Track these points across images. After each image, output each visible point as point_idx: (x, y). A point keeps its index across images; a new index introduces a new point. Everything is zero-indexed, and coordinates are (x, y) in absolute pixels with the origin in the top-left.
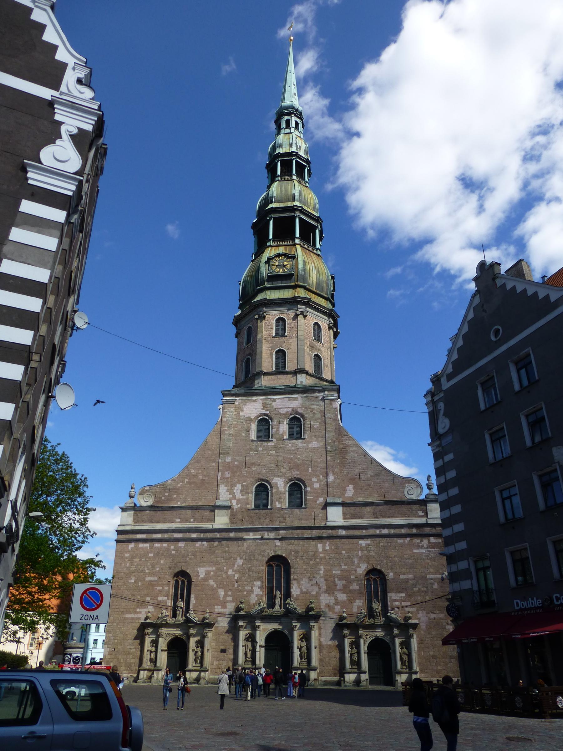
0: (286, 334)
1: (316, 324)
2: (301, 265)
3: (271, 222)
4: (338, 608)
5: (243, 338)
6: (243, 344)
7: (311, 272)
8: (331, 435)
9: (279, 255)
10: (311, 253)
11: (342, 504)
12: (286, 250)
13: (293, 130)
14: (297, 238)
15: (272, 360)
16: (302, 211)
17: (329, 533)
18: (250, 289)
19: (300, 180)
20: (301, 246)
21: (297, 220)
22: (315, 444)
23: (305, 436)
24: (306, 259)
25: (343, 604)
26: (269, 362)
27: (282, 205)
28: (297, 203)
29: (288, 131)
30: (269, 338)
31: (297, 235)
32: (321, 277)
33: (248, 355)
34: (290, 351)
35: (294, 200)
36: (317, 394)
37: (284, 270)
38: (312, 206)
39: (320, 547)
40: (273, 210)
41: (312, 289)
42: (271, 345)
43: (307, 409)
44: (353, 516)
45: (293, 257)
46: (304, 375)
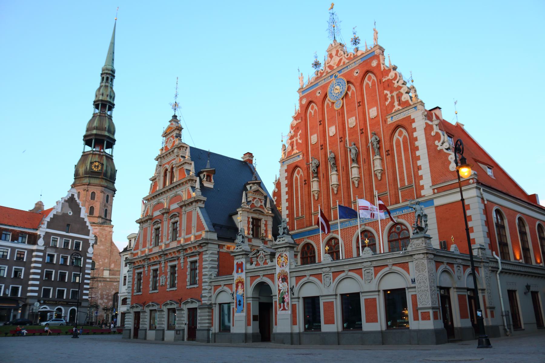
1: (108, 196)
2: (105, 168)
3: (93, 141)
4: (104, 304)
8: (108, 244)
11: (110, 270)
16: (109, 137)
17: (104, 280)
20: (107, 157)
21: (105, 142)
22: (102, 247)
23: (98, 244)
25: (106, 303)
27: (99, 132)
28: (106, 134)
29: (107, 84)
35: (105, 131)
36: (105, 228)
39: (100, 284)
40: (96, 135)
43: (100, 233)
44: (113, 275)
45: (102, 164)
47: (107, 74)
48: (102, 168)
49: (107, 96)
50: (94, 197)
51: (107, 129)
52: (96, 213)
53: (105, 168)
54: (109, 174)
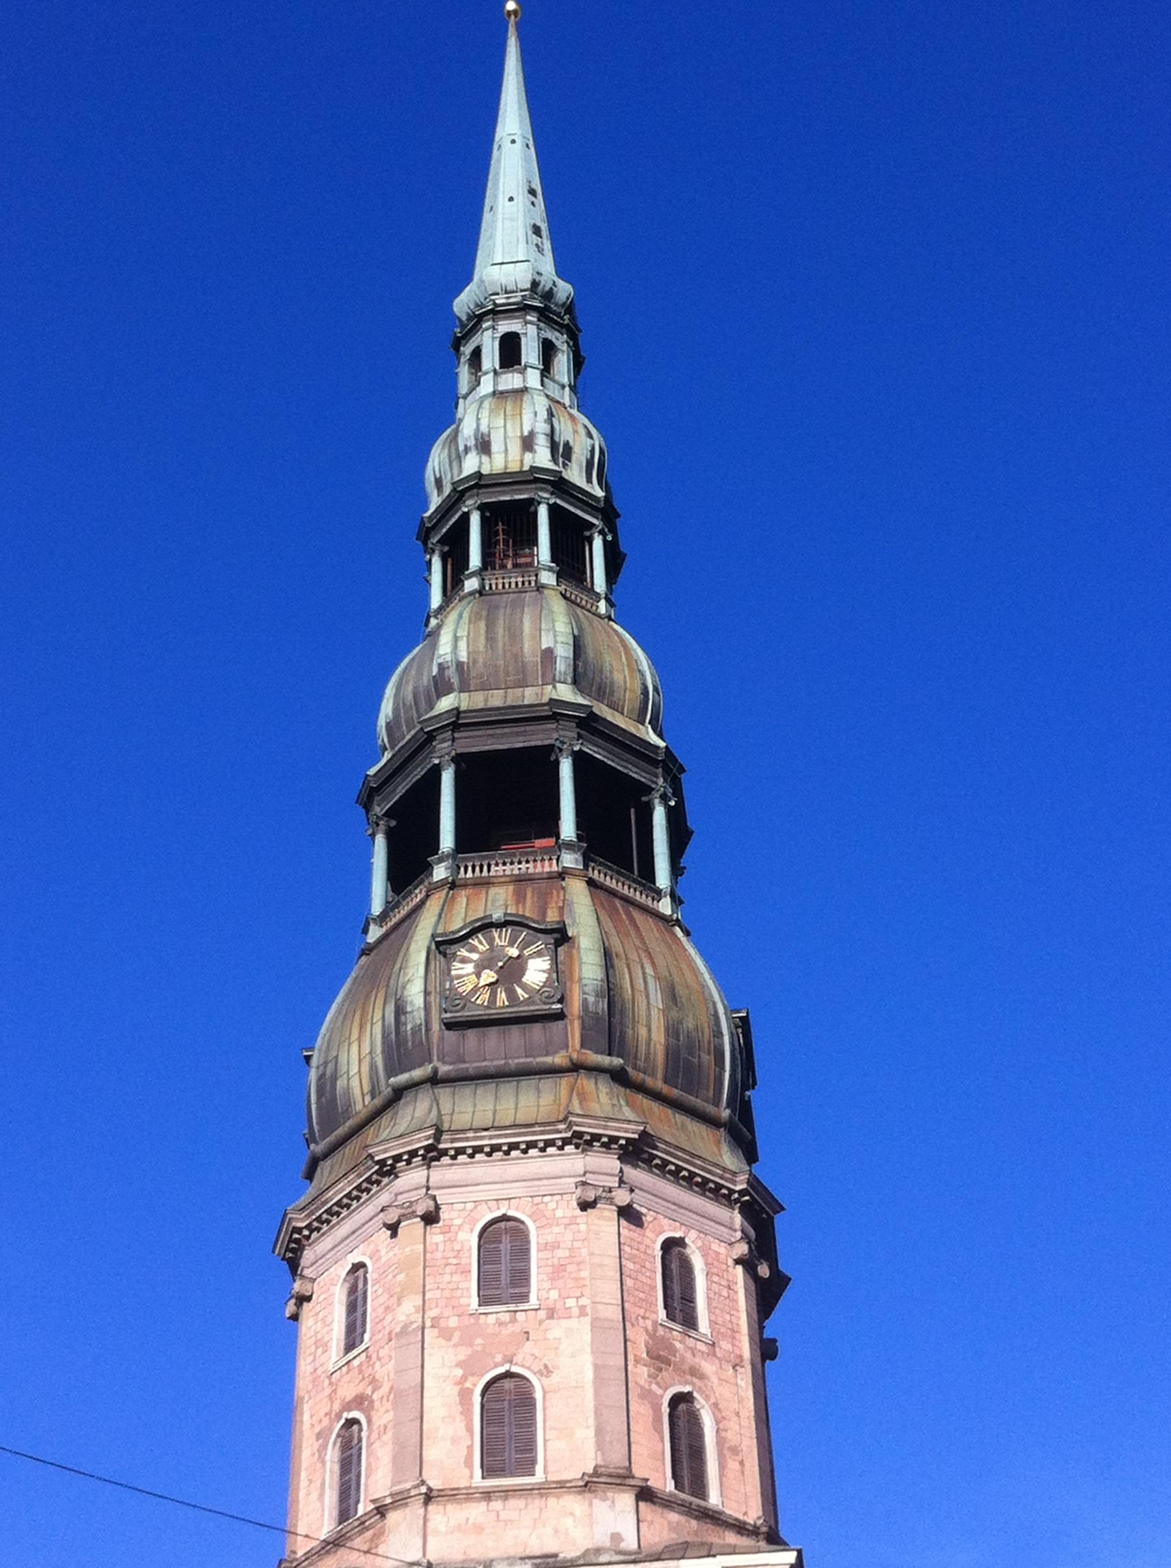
0: (533, 1297)
3: (447, 779)
5: (327, 1324)
6: (326, 1348)
7: (641, 1001)
9: (485, 926)
10: (637, 915)
12: (520, 898)
13: (533, 378)
14: (569, 846)
15: (470, 1429)
16: (589, 724)
18: (355, 1083)
19: (574, 593)
20: (591, 883)
21: (566, 769)
24: (616, 944)
26: (455, 1440)
28: (565, 692)
29: (511, 380)
30: (453, 1322)
31: (568, 828)
32: (689, 1023)
33: (347, 1407)
34: (555, 1378)
37: (511, 994)
38: (631, 699)
40: (457, 722)
41: (649, 1082)
42: (463, 1353)
45: (560, 937)
46: (626, 1500)
47: (496, 313)
48: (560, 973)
49: (528, 443)
50: (521, 1278)
51: (562, 666)
52: (567, 1438)
53: (588, 968)
54: (651, 1030)
